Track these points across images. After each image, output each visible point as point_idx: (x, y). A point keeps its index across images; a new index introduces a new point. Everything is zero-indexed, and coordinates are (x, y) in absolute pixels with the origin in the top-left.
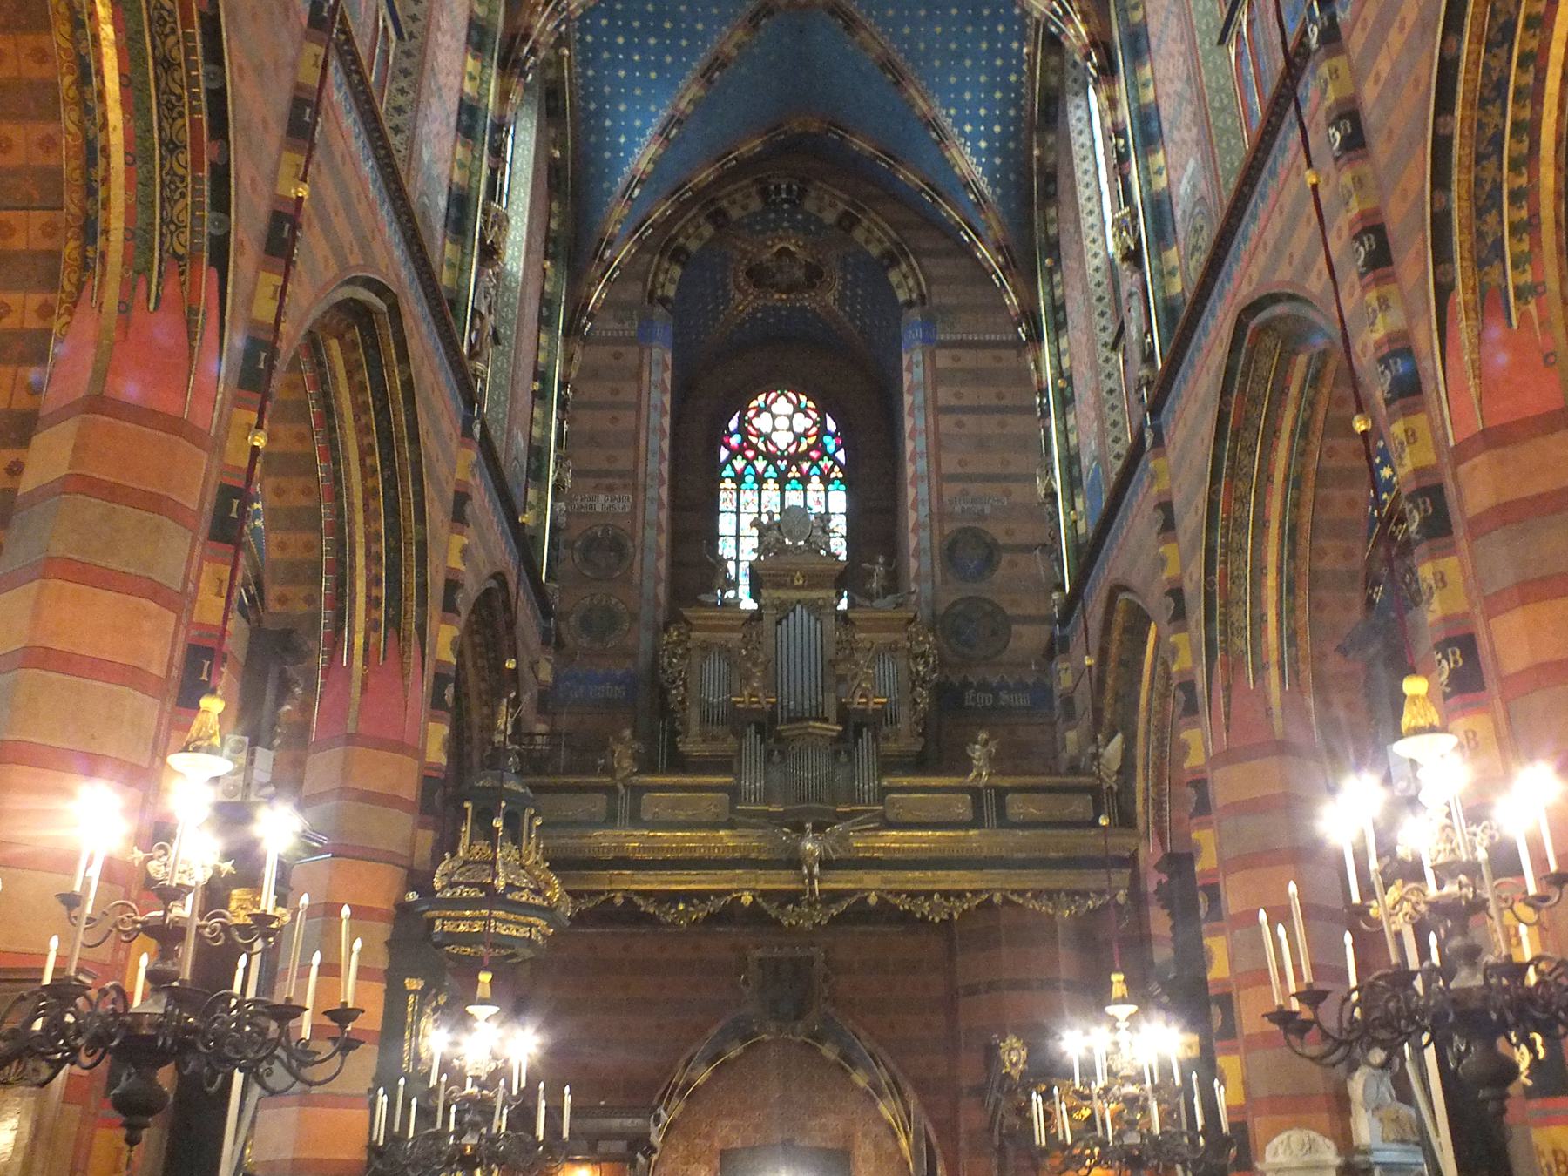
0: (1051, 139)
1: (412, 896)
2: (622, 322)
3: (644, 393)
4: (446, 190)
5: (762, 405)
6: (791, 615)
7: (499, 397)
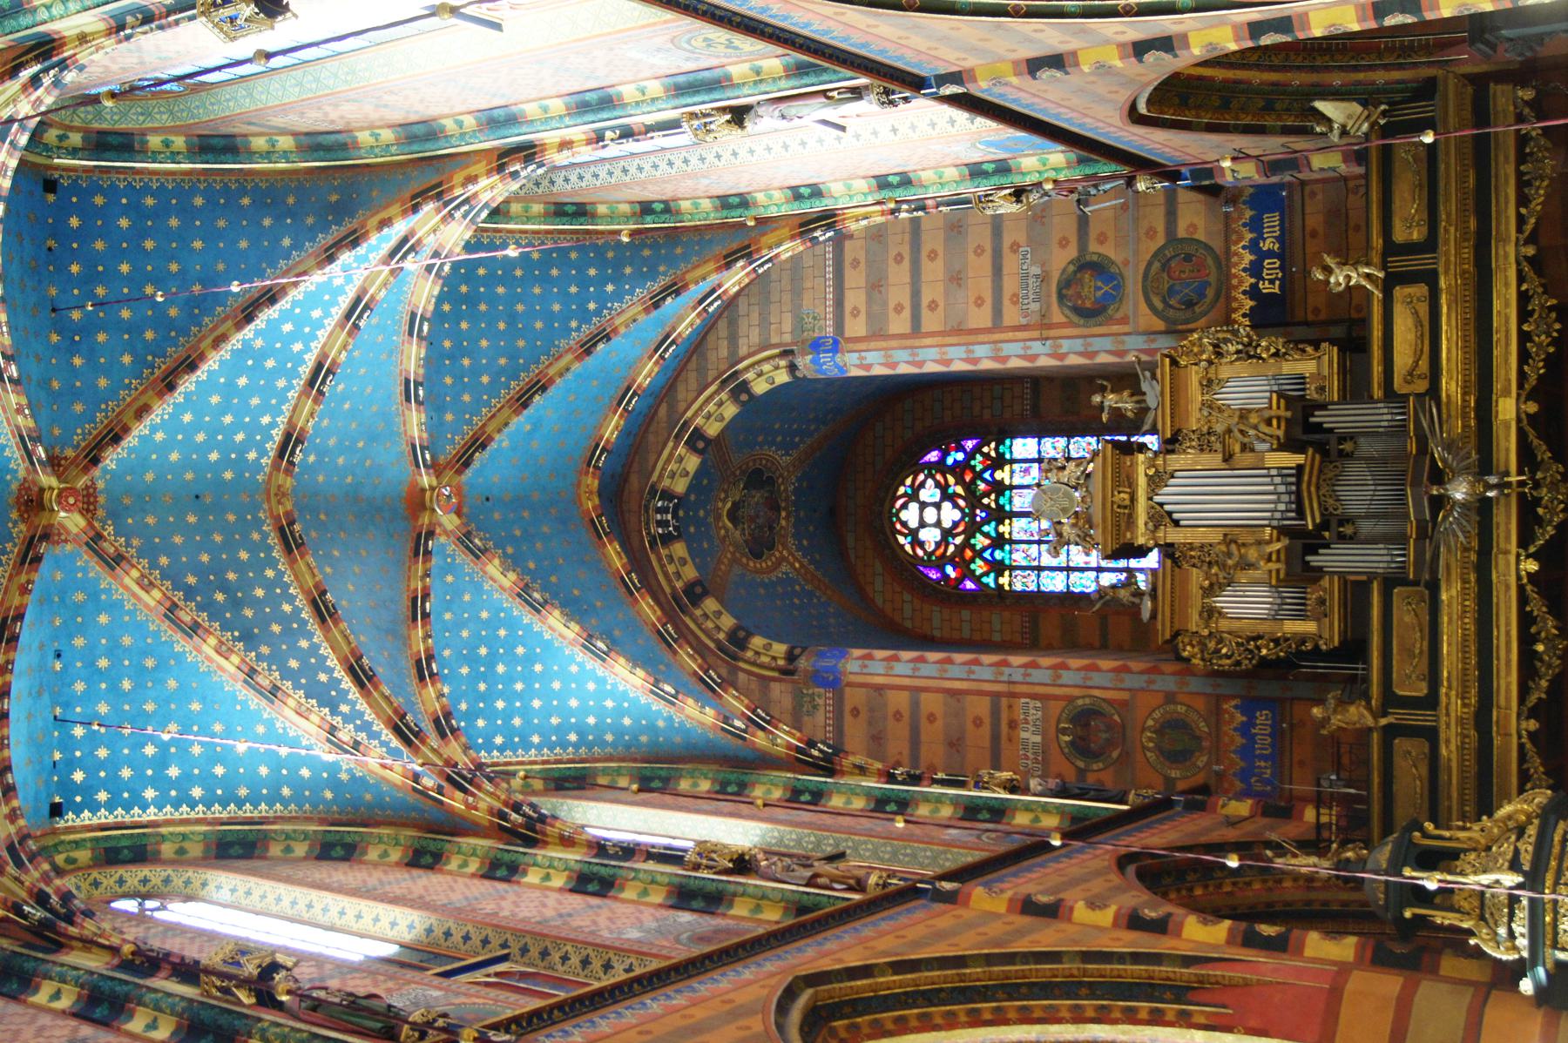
1: (1526, 986)
2: (815, 707)
3: (898, 681)
4: (672, 913)
5: (909, 539)
6: (1167, 507)
7: (906, 855)
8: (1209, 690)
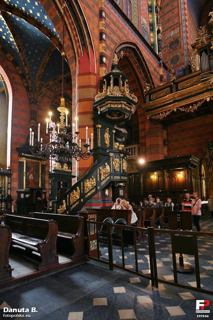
8: (185, 61)
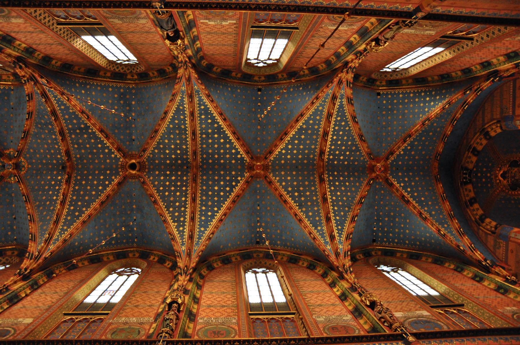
0: (430, 79)
